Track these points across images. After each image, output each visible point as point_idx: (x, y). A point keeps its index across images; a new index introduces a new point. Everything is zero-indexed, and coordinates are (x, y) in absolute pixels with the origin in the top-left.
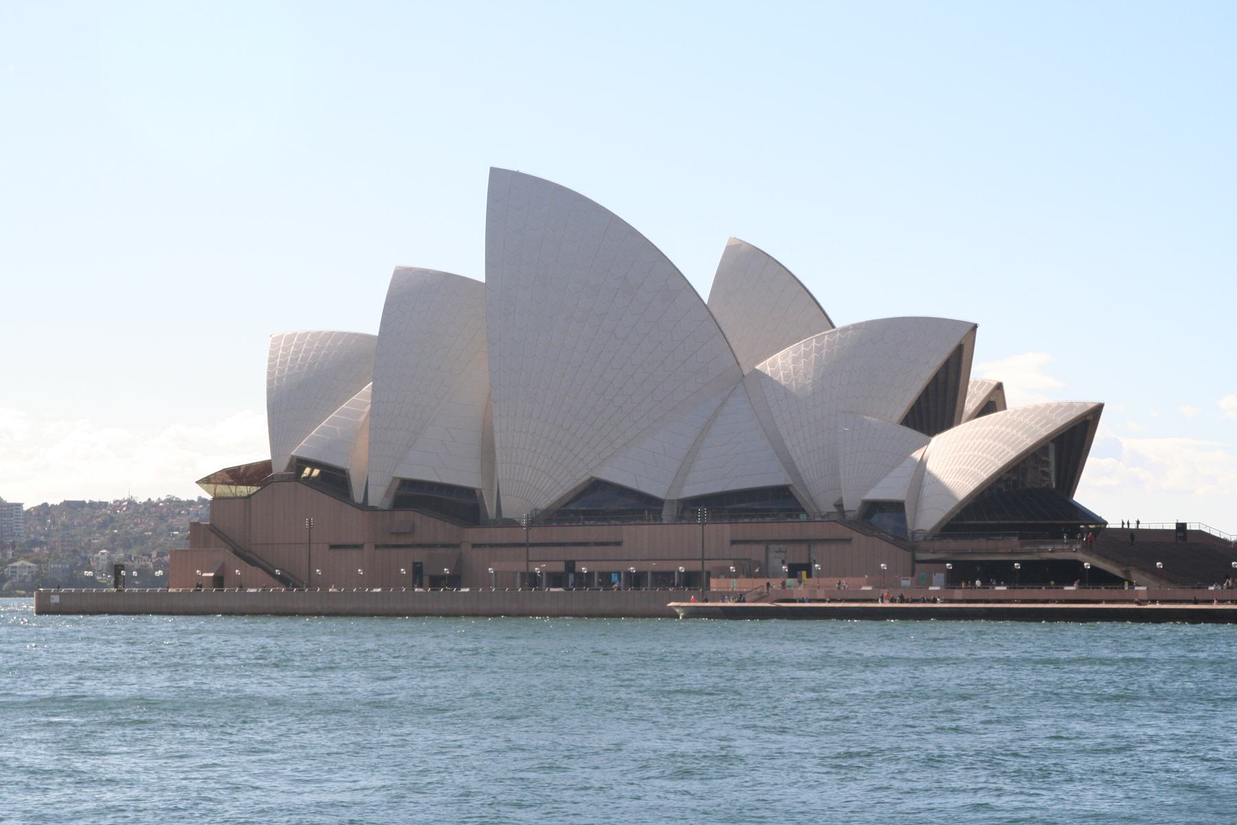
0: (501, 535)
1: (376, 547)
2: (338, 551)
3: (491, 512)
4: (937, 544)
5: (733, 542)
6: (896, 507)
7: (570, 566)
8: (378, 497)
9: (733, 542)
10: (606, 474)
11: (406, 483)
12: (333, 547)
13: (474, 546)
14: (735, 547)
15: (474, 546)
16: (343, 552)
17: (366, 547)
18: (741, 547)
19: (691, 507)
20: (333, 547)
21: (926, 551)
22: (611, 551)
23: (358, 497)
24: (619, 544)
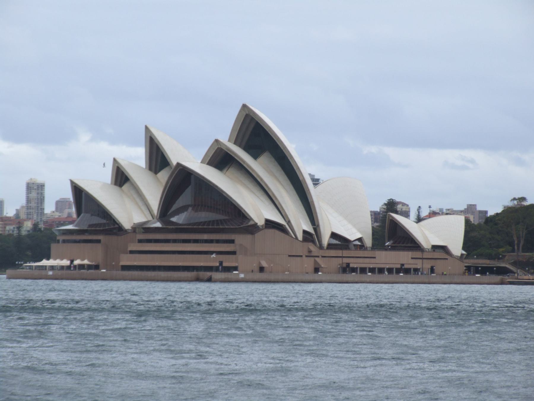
1: (306, 256)
2: (292, 258)
5: (412, 258)
8: (300, 236)
9: (412, 258)
12: (289, 256)
13: (323, 257)
15: (323, 257)
16: (294, 258)
17: (304, 256)
18: (414, 260)
20: (289, 256)
21: (467, 263)
22: (372, 260)
23: (294, 237)
24: (375, 258)
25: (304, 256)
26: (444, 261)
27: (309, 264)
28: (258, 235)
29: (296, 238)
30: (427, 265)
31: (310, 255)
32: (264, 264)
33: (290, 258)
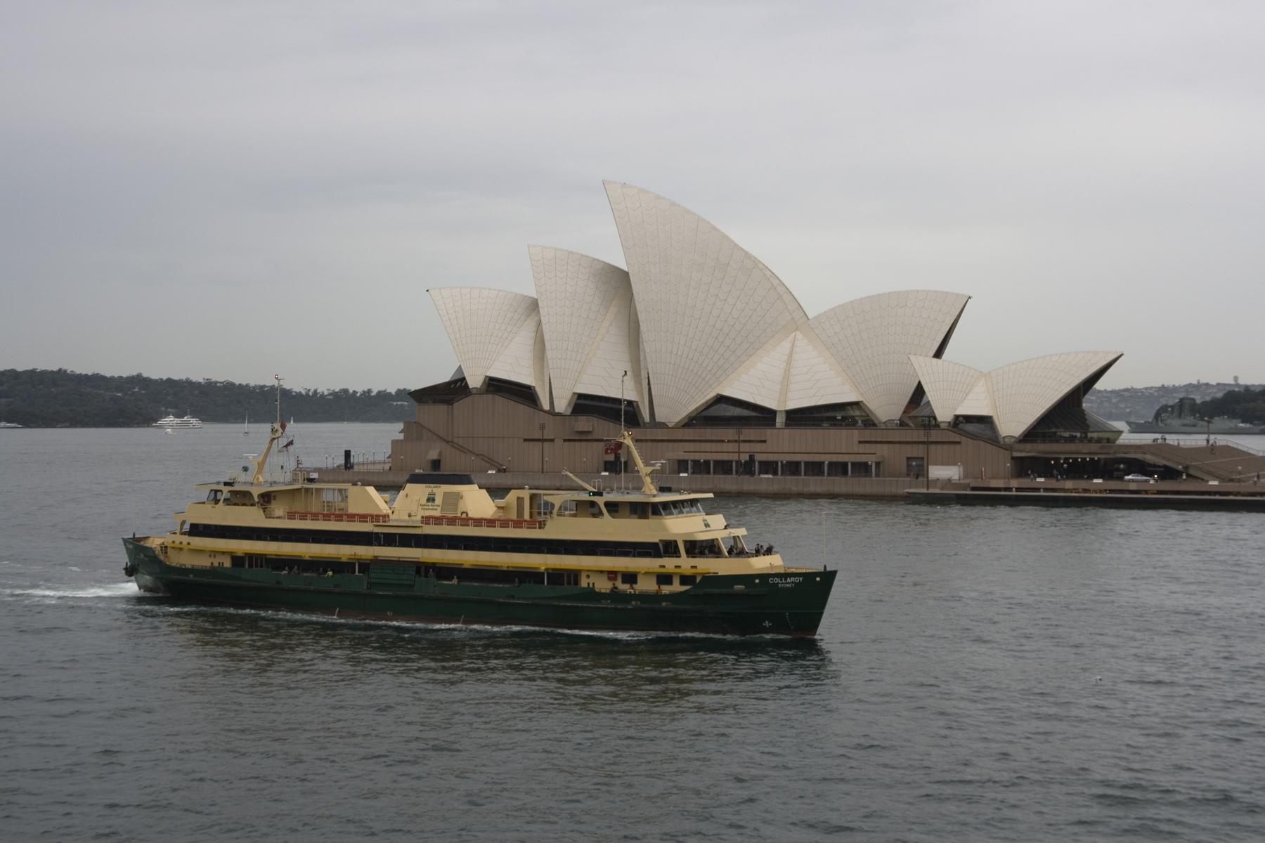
0: (660, 434)
3: (647, 418)
4: (1028, 446)
6: (985, 421)
7: (752, 457)
8: (562, 405)
10: (728, 392)
11: (581, 396)
14: (863, 448)
17: (559, 442)
19: (800, 417)
23: (546, 406)
24: (764, 441)
25: (559, 442)
26: (952, 446)
27: (593, 453)
28: (461, 406)
29: (552, 412)
30: (895, 456)
31: (583, 437)
32: (433, 455)
33: (526, 444)
